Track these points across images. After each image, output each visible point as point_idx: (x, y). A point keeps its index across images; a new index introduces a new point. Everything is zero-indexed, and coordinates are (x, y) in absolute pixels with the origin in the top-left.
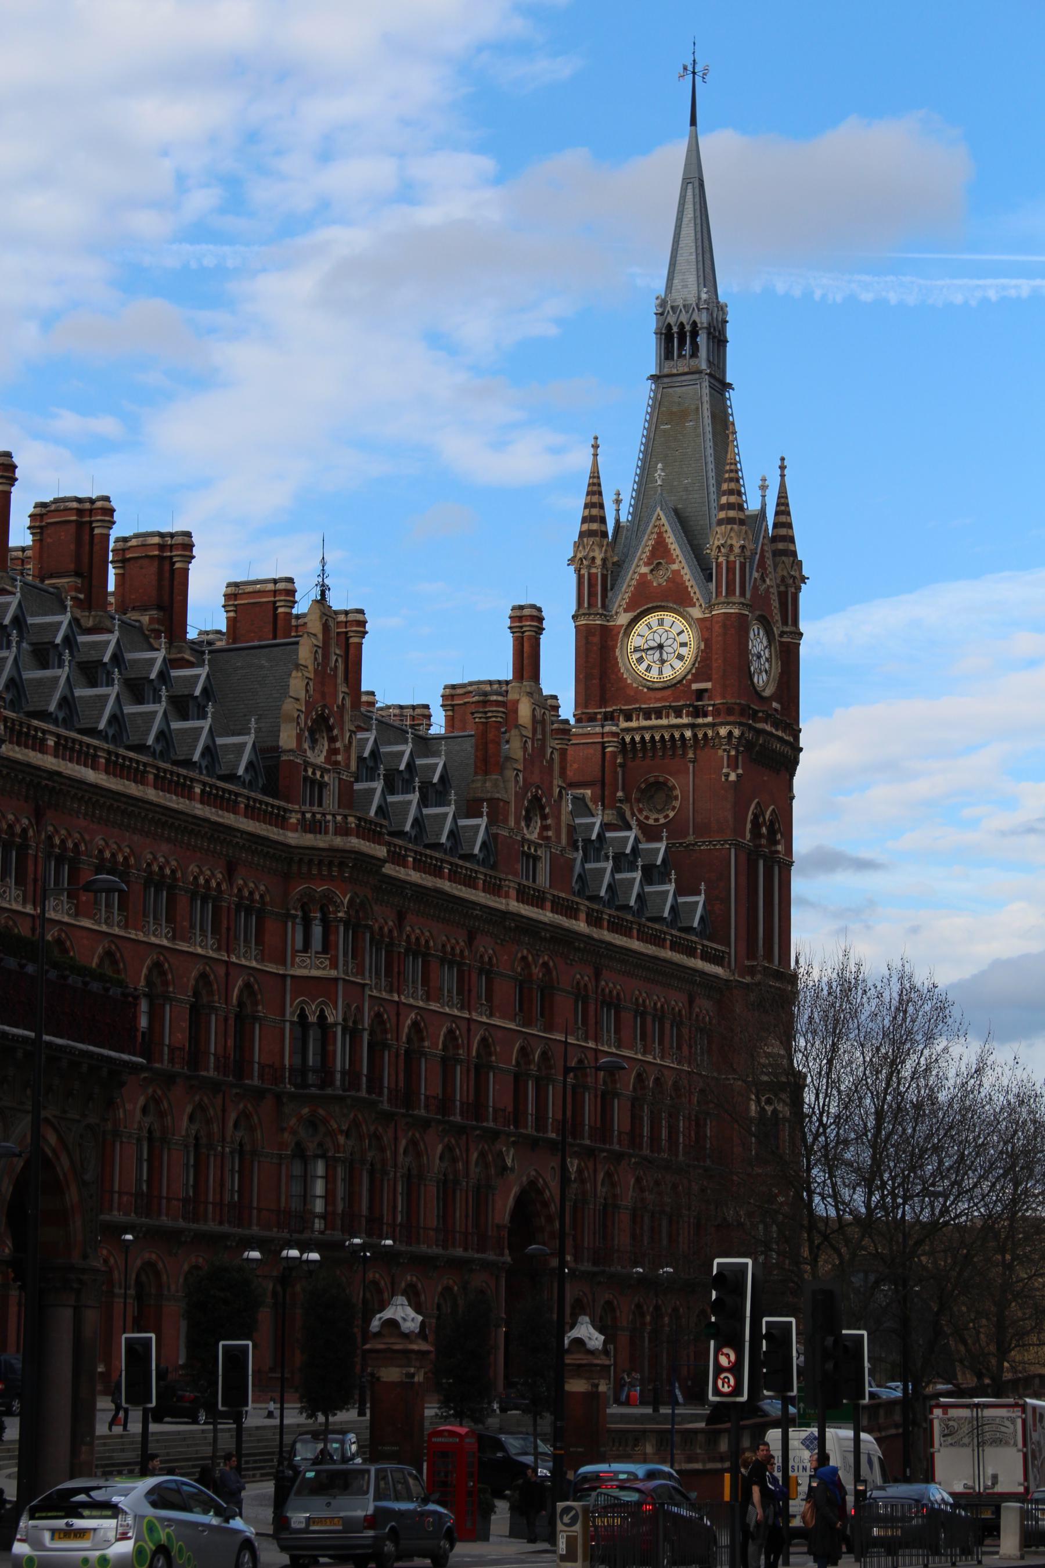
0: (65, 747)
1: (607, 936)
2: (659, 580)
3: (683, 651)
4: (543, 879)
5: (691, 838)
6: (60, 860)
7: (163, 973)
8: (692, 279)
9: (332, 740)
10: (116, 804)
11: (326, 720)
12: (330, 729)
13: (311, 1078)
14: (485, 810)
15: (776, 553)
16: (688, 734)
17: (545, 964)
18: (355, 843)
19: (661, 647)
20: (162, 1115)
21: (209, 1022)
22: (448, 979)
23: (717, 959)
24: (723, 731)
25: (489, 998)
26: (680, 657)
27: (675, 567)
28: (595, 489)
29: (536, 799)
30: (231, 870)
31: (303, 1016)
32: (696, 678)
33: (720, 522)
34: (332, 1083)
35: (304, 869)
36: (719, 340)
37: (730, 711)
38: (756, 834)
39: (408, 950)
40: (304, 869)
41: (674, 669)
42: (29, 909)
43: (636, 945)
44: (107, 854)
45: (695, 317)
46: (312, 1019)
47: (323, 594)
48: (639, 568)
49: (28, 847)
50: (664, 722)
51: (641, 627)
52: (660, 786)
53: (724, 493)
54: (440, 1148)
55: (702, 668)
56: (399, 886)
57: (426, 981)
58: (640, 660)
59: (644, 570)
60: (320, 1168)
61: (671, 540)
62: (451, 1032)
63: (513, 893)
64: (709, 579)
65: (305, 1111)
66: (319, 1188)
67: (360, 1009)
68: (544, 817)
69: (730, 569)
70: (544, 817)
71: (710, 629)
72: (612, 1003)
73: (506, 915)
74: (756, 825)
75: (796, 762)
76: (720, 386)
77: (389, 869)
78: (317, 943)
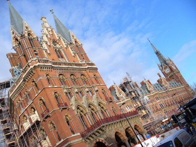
4: (169, 88)
22: (167, 97)
56: (160, 93)
77: (159, 93)
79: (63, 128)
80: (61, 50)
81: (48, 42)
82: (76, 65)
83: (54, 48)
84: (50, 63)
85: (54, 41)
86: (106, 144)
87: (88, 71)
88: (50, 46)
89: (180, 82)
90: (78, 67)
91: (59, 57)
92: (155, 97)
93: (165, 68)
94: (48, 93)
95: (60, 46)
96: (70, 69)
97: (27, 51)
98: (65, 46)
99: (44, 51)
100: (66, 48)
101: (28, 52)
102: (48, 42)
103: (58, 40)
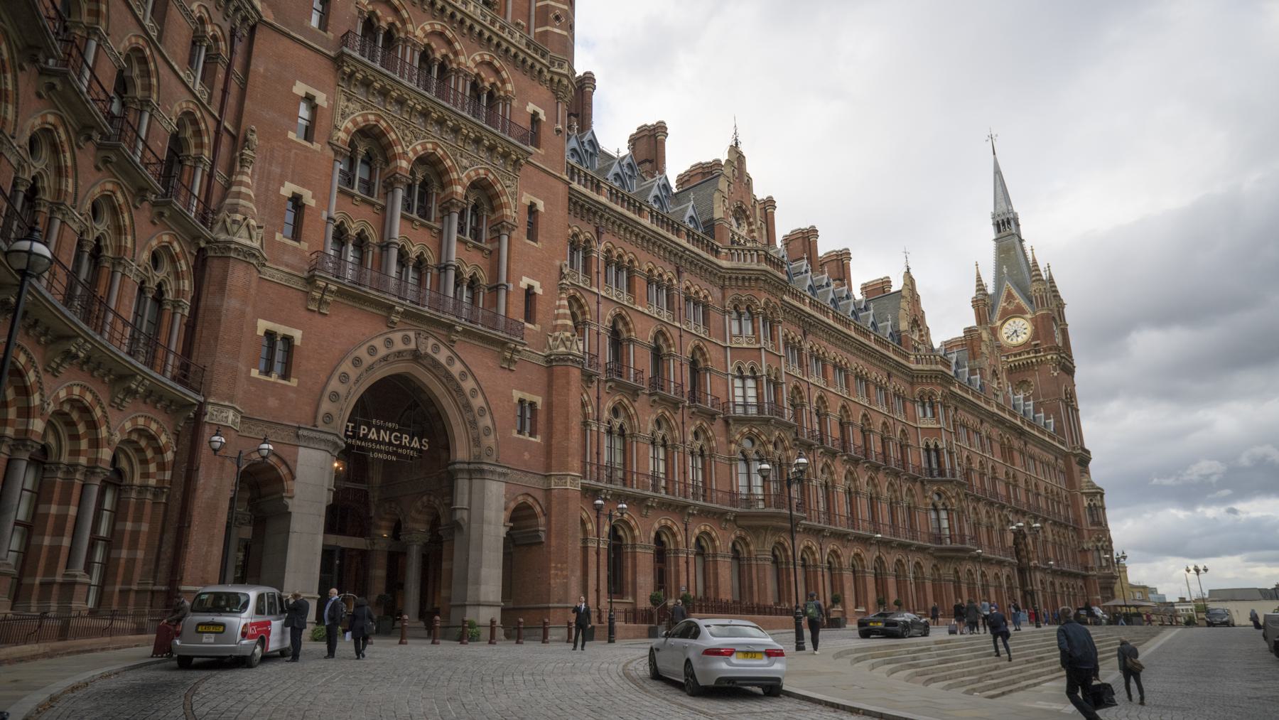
0: (814, 305)
1: (1027, 428)
2: (1011, 307)
3: (1025, 331)
5: (1041, 400)
6: (817, 360)
7: (868, 420)
8: (1004, 204)
9: (920, 331)
10: (839, 337)
11: (917, 321)
12: (919, 326)
13: (935, 473)
14: (978, 372)
15: (1054, 296)
16: (1034, 360)
17: (1008, 438)
18: (940, 367)
19: (1016, 331)
20: (875, 486)
21: (889, 445)
23: (1063, 444)
24: (1049, 357)
25: (992, 449)
26: (1025, 333)
27: (1017, 301)
28: (979, 279)
29: (994, 371)
30: (889, 376)
31: (927, 445)
32: (1033, 340)
33: (1034, 281)
34: (945, 476)
35: (920, 380)
36: (1017, 225)
37: (1051, 349)
38: (1067, 398)
39: (961, 425)
40: (920, 380)
41: (1022, 339)
42: (806, 378)
43: (1036, 433)
44: (838, 360)
45: (1008, 216)
46: (932, 447)
47: (908, 269)
48: (1002, 304)
49: (802, 349)
50: (1023, 357)
51: (1006, 325)
52: (1024, 382)
53: (1034, 276)
54: (984, 511)
55: (1035, 335)
57: (969, 439)
58: (1008, 337)
59: (1004, 304)
60: (943, 515)
61: (1014, 292)
62: (980, 462)
63: (995, 406)
64: (1032, 302)
65: (935, 488)
66: (945, 524)
67: (951, 443)
68: (998, 379)
69: (1041, 297)
70: (998, 379)
71: (1036, 321)
72: (1032, 457)
73: (994, 414)
74: (1066, 394)
75: (1074, 372)
76: (1021, 241)
78: (929, 414)
89: (1058, 421)
92: (918, 389)
93: (1006, 316)
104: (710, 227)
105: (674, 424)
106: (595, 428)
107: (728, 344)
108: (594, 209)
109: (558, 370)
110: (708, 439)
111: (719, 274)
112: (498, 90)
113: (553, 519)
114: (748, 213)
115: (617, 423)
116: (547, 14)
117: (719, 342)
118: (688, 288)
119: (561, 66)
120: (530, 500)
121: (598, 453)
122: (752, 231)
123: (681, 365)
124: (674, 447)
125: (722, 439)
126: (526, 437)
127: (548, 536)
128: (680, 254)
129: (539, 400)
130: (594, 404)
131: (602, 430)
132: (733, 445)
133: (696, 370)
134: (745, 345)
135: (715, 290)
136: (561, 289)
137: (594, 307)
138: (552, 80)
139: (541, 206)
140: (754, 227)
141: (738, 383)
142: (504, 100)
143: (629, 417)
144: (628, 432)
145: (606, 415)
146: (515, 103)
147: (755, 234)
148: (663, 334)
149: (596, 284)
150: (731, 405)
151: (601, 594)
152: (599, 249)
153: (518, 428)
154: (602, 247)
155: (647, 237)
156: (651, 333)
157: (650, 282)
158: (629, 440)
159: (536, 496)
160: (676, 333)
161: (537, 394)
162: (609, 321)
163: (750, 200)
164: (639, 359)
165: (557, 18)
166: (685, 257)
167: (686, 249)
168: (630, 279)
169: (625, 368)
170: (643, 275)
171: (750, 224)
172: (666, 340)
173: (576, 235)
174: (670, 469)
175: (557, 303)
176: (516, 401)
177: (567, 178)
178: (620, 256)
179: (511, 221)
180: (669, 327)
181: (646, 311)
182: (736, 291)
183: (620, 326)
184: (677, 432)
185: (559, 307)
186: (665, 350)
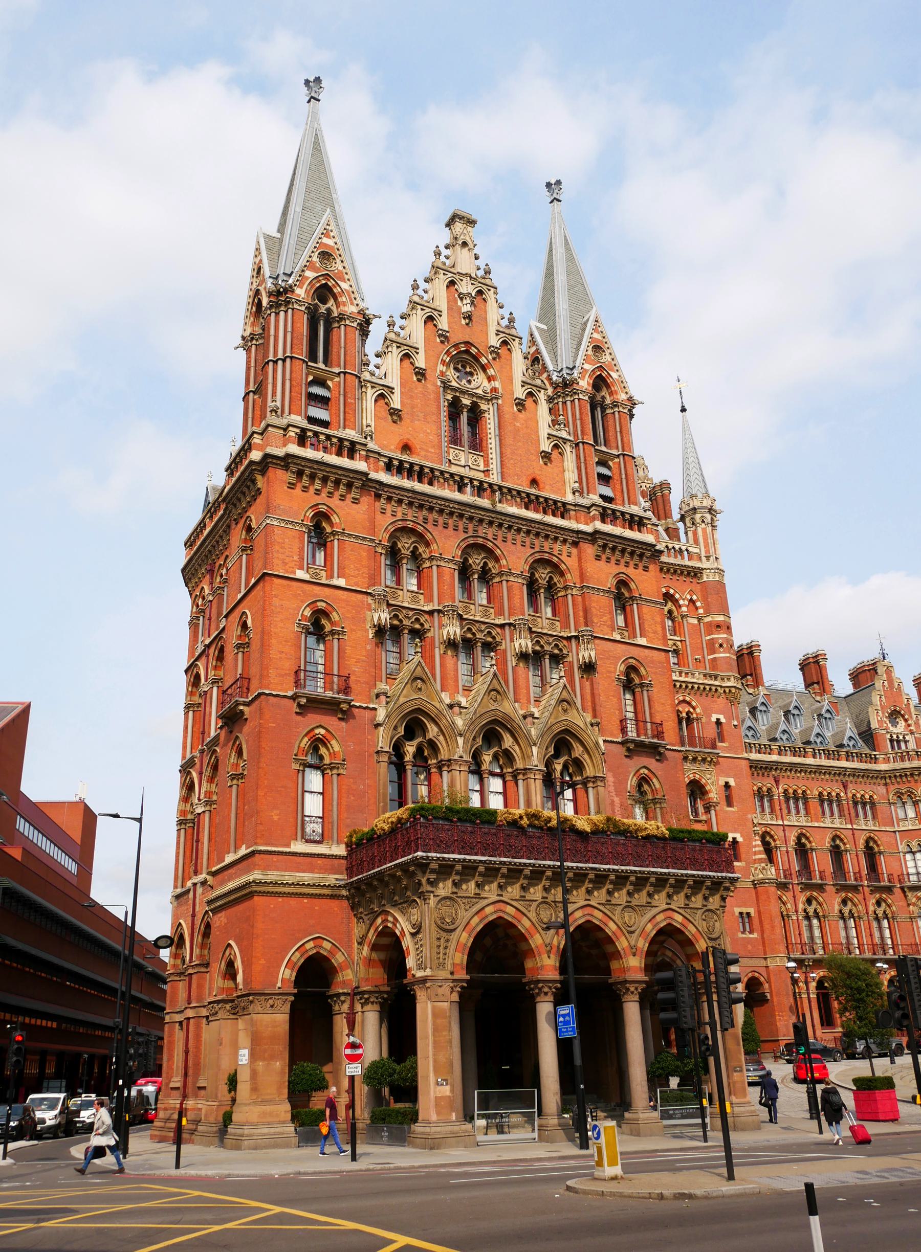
79: (260, 793)
80: (484, 407)
81: (422, 351)
82: (529, 501)
83: (446, 386)
84: (367, 458)
85: (467, 352)
86: (410, 962)
87: (589, 550)
88: (421, 374)
90: (538, 516)
91: (455, 440)
94: (276, 602)
95: (487, 386)
96: (479, 514)
97: (275, 371)
98: (520, 393)
99: (370, 391)
100: (520, 404)
101: (275, 378)
102: (422, 351)
103: (495, 352)
104: (868, 736)
105: (856, 901)
106: (795, 918)
107: (896, 829)
108: (769, 766)
109: (761, 889)
110: (889, 906)
111: (880, 776)
112: (692, 714)
113: (772, 984)
114: (902, 712)
115: (811, 910)
116: (714, 645)
117: (888, 829)
118: (854, 795)
119: (729, 679)
120: (756, 975)
121: (800, 934)
122: (909, 725)
123: (857, 856)
124: (860, 918)
125: (903, 903)
126: (748, 935)
127: (771, 996)
128: (843, 773)
129: (752, 911)
130: (792, 901)
131: (800, 918)
132: (911, 907)
133: (871, 854)
134: (910, 828)
135: (879, 788)
136: (755, 834)
137: (782, 834)
138: (725, 691)
139: (732, 782)
140: (910, 722)
141: (908, 857)
142: (697, 720)
143: (820, 904)
144: (821, 914)
145: (801, 907)
146: (704, 720)
147: (912, 728)
148: (838, 837)
149: (780, 817)
150: (906, 876)
151: (816, 1027)
152: (778, 792)
153: (742, 929)
154: (781, 790)
155: (814, 770)
156: (828, 839)
157: (822, 801)
158: (822, 919)
159: (760, 972)
160: (851, 832)
161: (750, 906)
162: (793, 841)
163: (903, 701)
164: (821, 862)
165: (721, 645)
166: (847, 773)
167: (846, 768)
168: (806, 803)
169: (812, 873)
170: (815, 798)
171: (906, 720)
172: (841, 840)
173: (760, 788)
174: (859, 934)
175: (754, 843)
176: (737, 914)
177: (745, 755)
178: (795, 791)
179: (715, 800)
180: (841, 830)
181: (822, 825)
182: (897, 786)
183: (804, 840)
184: (860, 906)
185: (755, 846)
186: (843, 847)
